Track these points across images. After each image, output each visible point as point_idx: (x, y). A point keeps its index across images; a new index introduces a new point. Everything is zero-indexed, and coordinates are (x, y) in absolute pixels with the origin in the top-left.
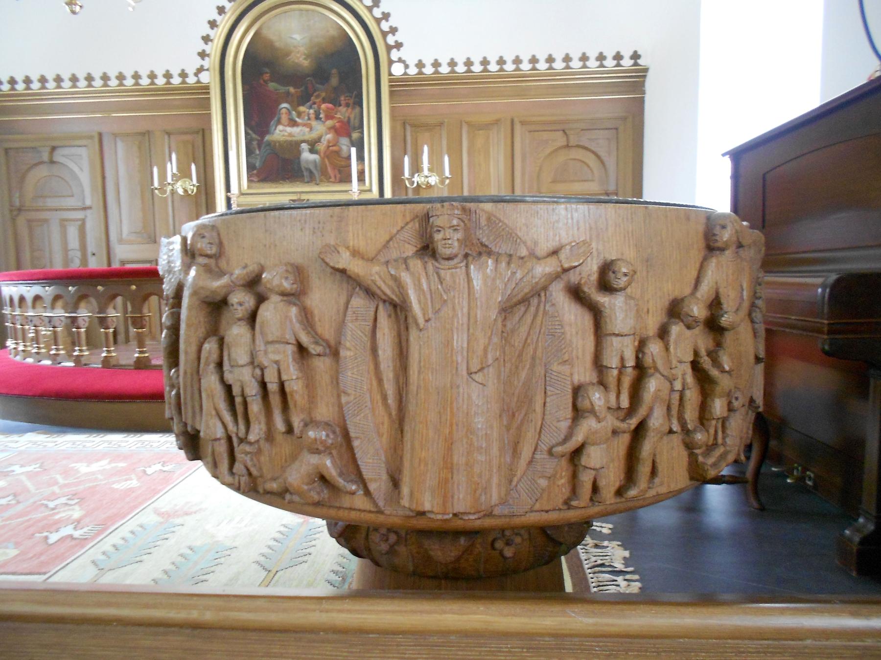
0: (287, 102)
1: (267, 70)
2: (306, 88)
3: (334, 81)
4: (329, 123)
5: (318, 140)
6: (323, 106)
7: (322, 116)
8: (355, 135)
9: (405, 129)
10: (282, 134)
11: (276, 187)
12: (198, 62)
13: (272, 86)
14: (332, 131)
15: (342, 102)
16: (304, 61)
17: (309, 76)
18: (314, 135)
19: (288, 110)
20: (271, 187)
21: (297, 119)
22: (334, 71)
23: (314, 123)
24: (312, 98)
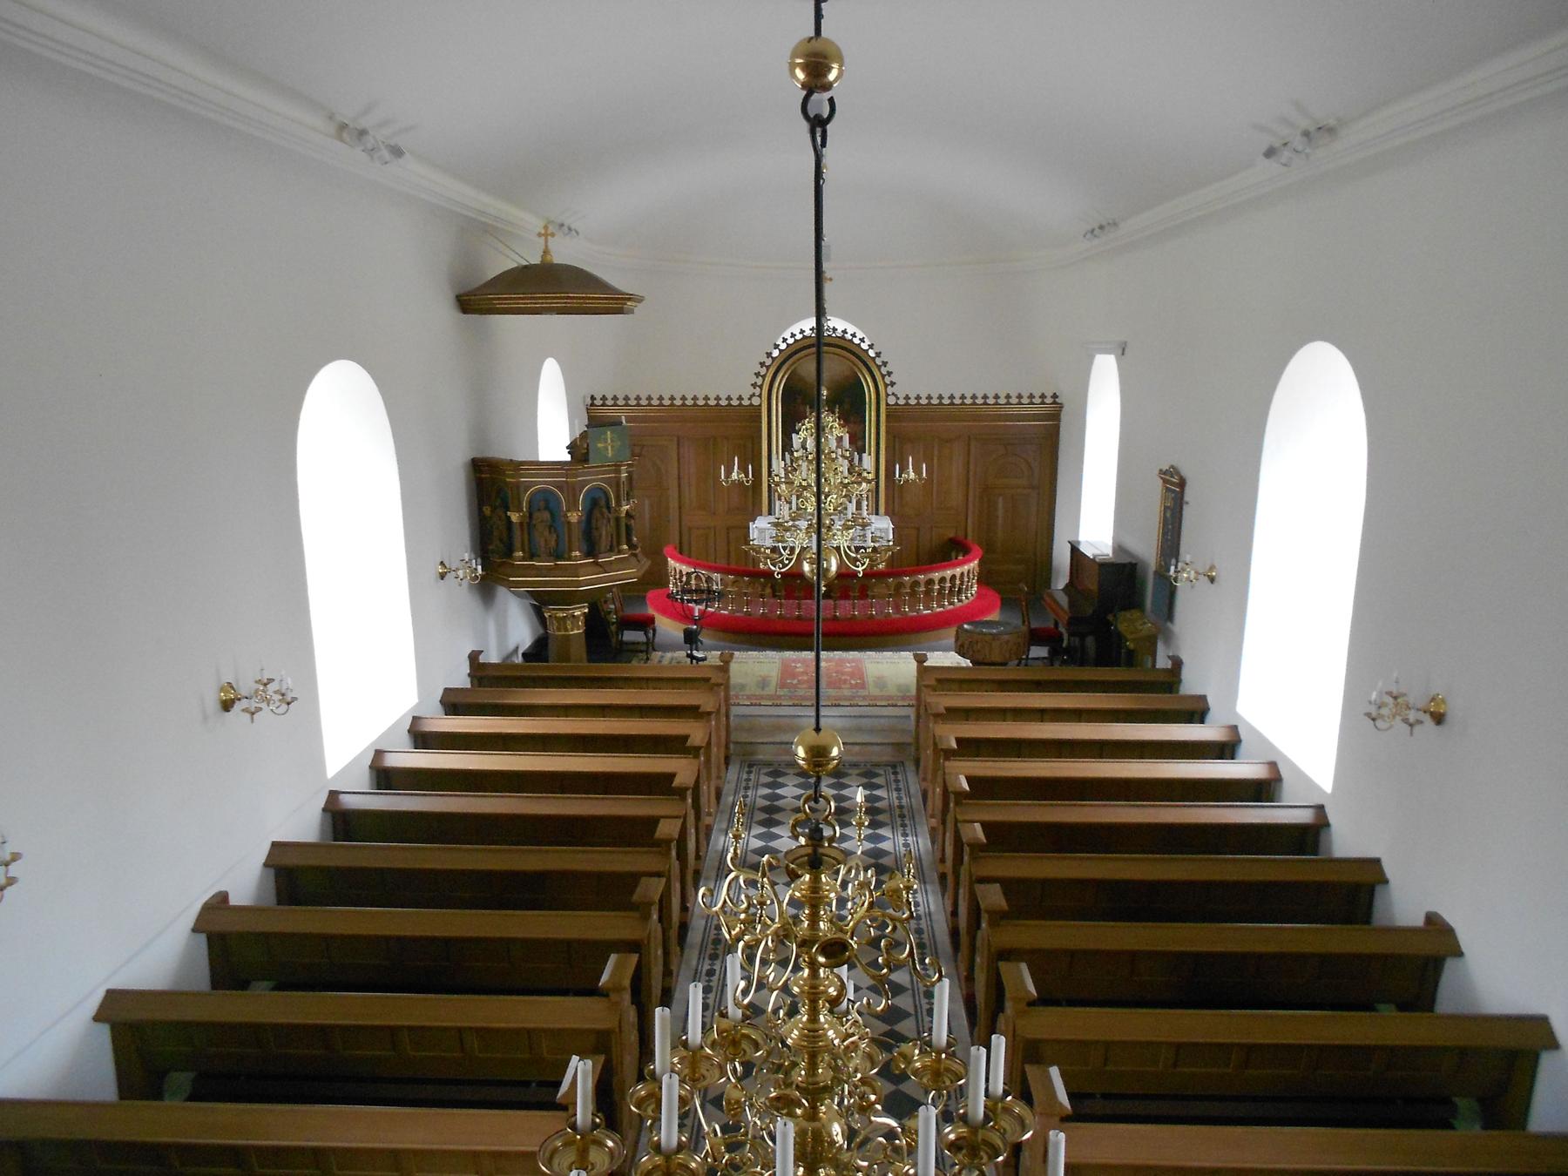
8: (860, 443)
9: (894, 441)
12: (752, 390)
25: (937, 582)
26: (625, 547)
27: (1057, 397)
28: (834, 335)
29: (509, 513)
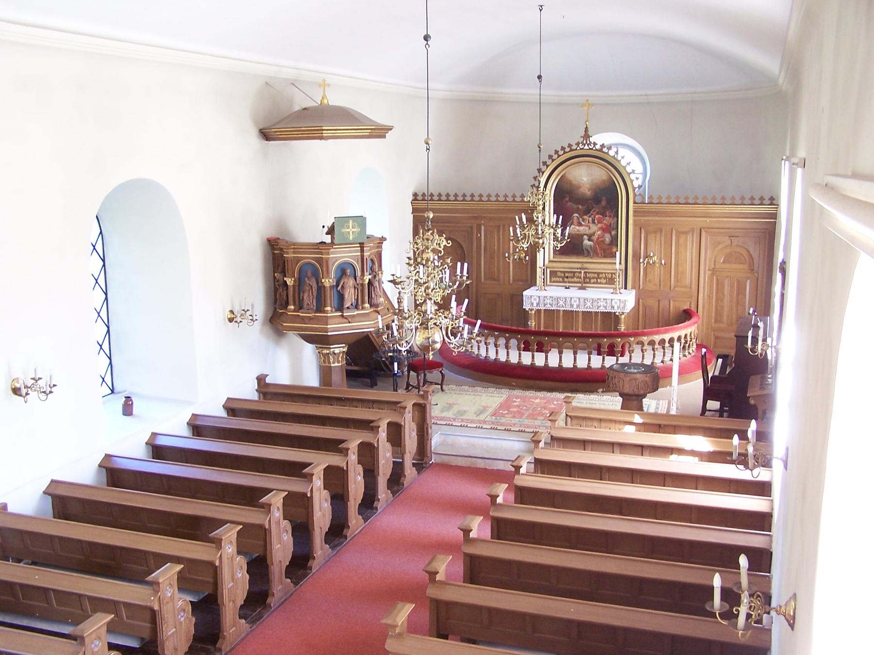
0: (577, 213)
1: (567, 195)
2: (588, 207)
3: (604, 203)
4: (600, 225)
5: (594, 234)
6: (597, 216)
7: (596, 221)
8: (613, 233)
10: (574, 230)
11: (569, 258)
13: (570, 204)
14: (601, 230)
15: (607, 215)
16: (588, 192)
17: (590, 200)
18: (591, 231)
19: (577, 217)
20: (566, 258)
21: (582, 223)
22: (604, 198)
23: (591, 225)
24: (591, 212)
25: (657, 343)
26: (367, 305)
27: (774, 199)
28: (594, 149)
29: (285, 279)
